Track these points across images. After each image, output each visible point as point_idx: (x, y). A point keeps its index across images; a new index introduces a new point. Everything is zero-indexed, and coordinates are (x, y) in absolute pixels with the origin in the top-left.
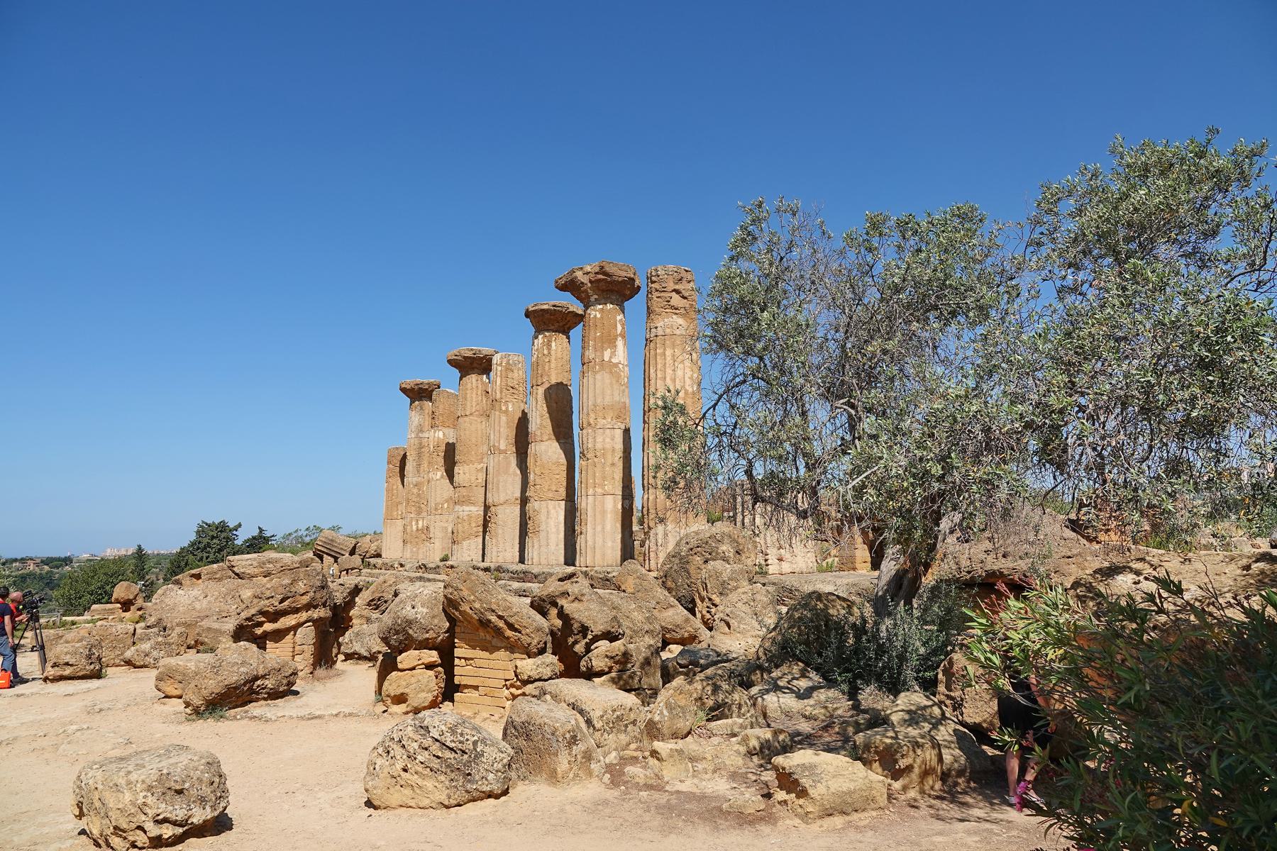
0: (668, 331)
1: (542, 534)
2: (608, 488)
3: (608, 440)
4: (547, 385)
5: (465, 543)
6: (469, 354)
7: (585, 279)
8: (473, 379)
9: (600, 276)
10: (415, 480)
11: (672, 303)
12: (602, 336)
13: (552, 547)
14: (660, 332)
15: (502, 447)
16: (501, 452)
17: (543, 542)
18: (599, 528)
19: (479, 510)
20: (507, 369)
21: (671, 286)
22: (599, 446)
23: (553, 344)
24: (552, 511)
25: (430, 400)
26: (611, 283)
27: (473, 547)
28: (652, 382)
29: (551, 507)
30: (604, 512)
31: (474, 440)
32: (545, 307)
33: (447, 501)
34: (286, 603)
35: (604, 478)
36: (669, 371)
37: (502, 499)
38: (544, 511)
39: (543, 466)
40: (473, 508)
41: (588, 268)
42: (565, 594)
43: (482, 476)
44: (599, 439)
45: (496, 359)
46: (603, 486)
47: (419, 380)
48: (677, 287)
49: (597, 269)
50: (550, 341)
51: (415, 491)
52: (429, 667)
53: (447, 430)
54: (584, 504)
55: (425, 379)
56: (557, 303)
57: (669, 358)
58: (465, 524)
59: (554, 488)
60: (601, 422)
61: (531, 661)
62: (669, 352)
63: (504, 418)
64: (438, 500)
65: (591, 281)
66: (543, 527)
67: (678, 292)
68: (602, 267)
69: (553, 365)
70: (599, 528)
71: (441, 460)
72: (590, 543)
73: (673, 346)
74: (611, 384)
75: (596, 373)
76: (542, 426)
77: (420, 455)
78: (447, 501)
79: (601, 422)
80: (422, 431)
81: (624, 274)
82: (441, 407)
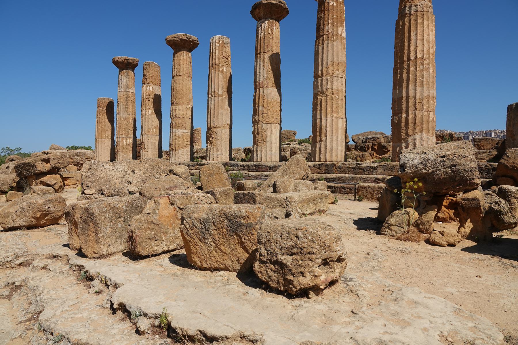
1: (268, 144)
3: (340, 84)
4: (270, 53)
5: (180, 151)
6: (184, 37)
8: (184, 56)
10: (124, 116)
12: (337, 18)
13: (273, 151)
14: (419, 9)
15: (220, 93)
17: (268, 149)
18: (334, 138)
19: (187, 132)
20: (222, 46)
22: (335, 88)
23: (274, 28)
24: (274, 130)
25: (133, 70)
27: (185, 153)
28: (413, 42)
29: (273, 127)
30: (337, 129)
31: (185, 90)
32: (274, 2)
35: (337, 108)
36: (426, 36)
37: (220, 125)
38: (269, 130)
39: (268, 103)
40: (185, 131)
43: (190, 113)
44: (335, 83)
46: (337, 113)
47: (127, 57)
50: (272, 26)
51: (125, 122)
53: (154, 86)
54: (323, 123)
57: (425, 27)
58: (181, 140)
62: (426, 23)
64: (150, 127)
66: (268, 139)
69: (274, 41)
70: (334, 138)
71: (151, 104)
72: (328, 147)
74: (341, 49)
75: (333, 41)
76: (267, 78)
77: (127, 102)
79: (336, 73)
80: (128, 88)
82: (151, 72)
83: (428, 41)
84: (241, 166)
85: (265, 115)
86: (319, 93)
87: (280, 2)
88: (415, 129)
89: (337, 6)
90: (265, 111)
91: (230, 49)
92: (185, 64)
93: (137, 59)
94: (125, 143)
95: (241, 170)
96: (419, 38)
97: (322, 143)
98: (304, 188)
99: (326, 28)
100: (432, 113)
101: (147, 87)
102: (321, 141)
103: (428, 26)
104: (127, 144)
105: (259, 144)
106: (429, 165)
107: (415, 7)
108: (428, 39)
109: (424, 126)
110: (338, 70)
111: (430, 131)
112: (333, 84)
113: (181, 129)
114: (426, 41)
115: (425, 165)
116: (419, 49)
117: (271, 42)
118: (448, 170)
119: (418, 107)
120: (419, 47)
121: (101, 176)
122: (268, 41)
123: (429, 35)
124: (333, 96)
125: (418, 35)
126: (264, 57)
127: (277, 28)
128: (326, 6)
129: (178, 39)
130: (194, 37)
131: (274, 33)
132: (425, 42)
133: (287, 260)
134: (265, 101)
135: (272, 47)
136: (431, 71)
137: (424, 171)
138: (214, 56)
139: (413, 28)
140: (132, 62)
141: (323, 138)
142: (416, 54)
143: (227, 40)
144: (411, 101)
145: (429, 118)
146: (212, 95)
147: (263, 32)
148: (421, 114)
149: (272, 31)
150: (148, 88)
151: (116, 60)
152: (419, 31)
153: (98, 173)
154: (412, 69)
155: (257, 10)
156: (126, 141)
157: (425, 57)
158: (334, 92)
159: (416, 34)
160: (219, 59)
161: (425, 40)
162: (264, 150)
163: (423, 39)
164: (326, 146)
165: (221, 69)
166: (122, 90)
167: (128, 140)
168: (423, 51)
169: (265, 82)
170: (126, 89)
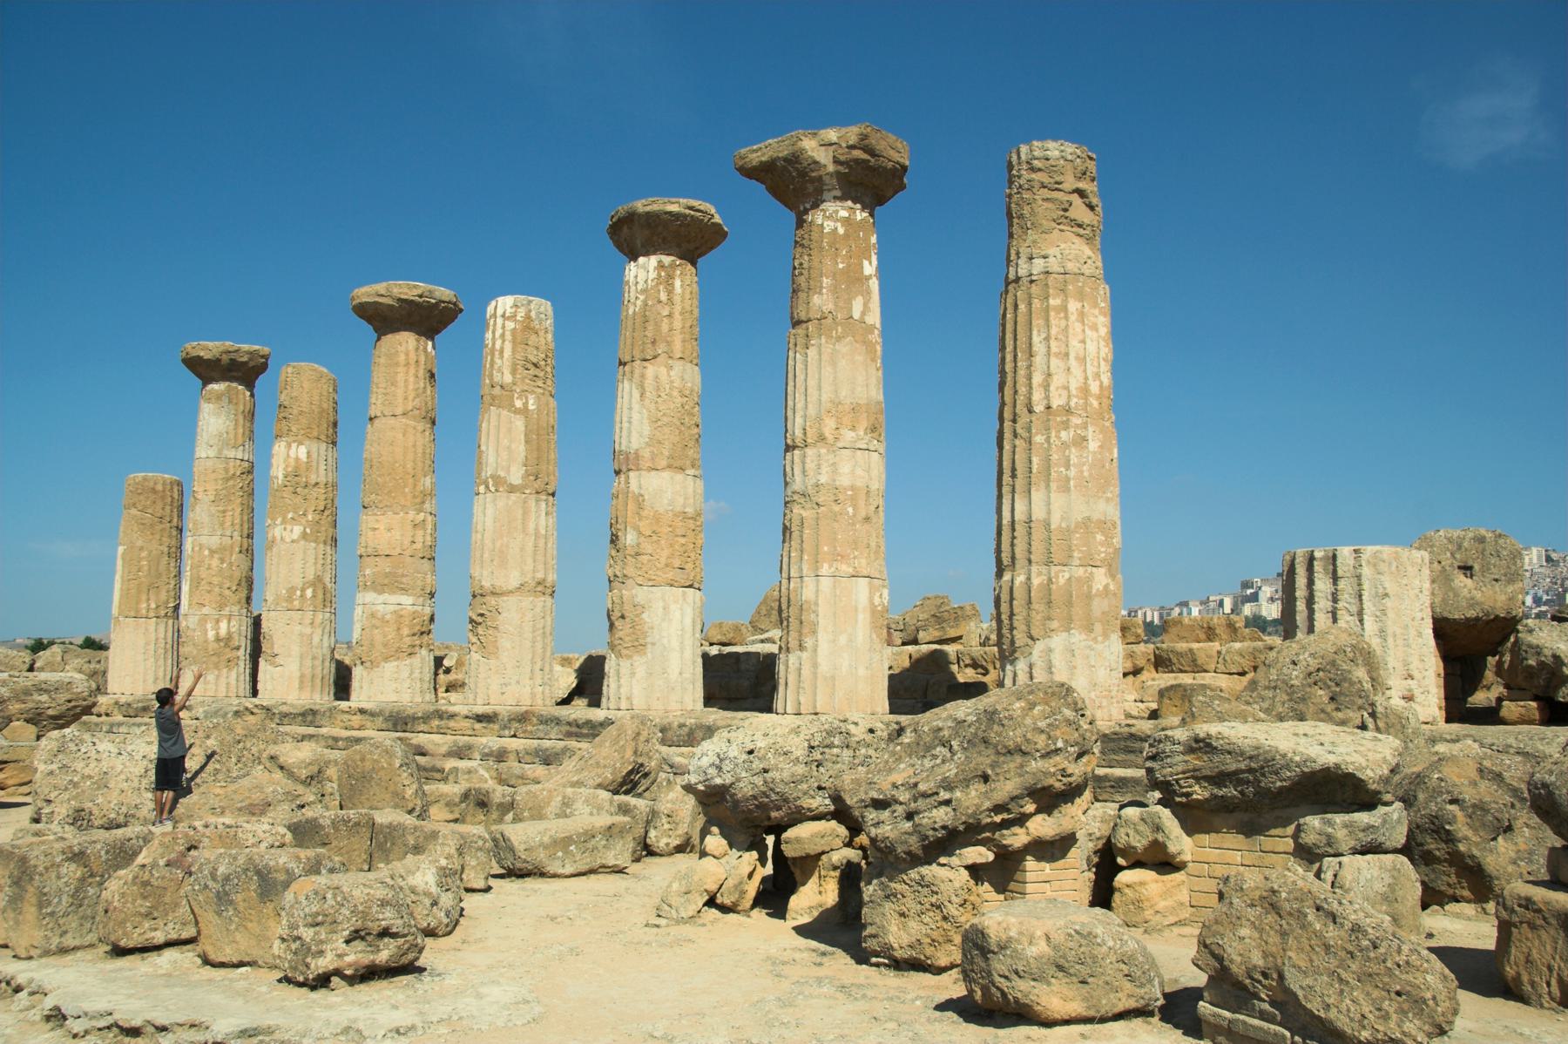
0: (1070, 266)
2: (862, 564)
3: (859, 472)
7: (824, 157)
9: (858, 154)
11: (1071, 214)
16: (512, 489)
21: (1070, 183)
23: (678, 283)
24: (673, 607)
26: (874, 170)
28: (1039, 360)
33: (313, 584)
36: (1075, 343)
37: (514, 582)
39: (657, 518)
44: (845, 469)
48: (1081, 185)
49: (853, 140)
50: (671, 277)
53: (314, 446)
56: (695, 203)
57: (1073, 318)
59: (677, 563)
60: (848, 436)
62: (1073, 306)
63: (519, 423)
65: (836, 161)
67: (1081, 193)
68: (864, 137)
69: (677, 324)
73: (1081, 296)
78: (313, 584)
83: (1082, 360)
84: (569, 724)
85: (645, 558)
86: (796, 497)
87: (691, 208)
88: (1049, 619)
89: (847, 236)
90: (647, 547)
91: (550, 337)
92: (412, 379)
93: (266, 350)
94: (211, 634)
95: (569, 735)
96: (1054, 349)
98: (588, 810)
99: (816, 300)
100: (1102, 570)
101: (289, 446)
102: (801, 647)
103: (1082, 315)
104: (218, 639)
105: (624, 652)
106: (725, 768)
107: (1041, 261)
108: (1081, 354)
109: (1078, 611)
110: (853, 428)
111: (1098, 627)
112: (835, 472)
113: (392, 592)
114: (1077, 358)
115: (719, 768)
116: (1057, 381)
117: (665, 327)
118: (759, 781)
119: (1056, 558)
120: (1055, 378)
121: (87, 771)
122: (657, 326)
123: (1083, 342)
124: (837, 508)
125: (1053, 344)
126: (643, 376)
127: (684, 280)
128: (815, 236)
129: (390, 302)
130: (444, 293)
131: (677, 299)
132: (1073, 362)
133: (307, 934)
134: (644, 513)
135: (668, 343)
136: (1093, 445)
137: (718, 781)
138: (499, 362)
139: (1038, 322)
140: (245, 359)
141: (809, 642)
142: (1047, 397)
143: (541, 308)
144: (1038, 535)
145: (1090, 587)
146: (487, 487)
148: (1067, 575)
149: (670, 292)
150: (292, 453)
151: (194, 353)
152: (1054, 331)
153: (79, 765)
154: (1039, 439)
155: (625, 229)
156: (217, 629)
157: (1072, 404)
158: (841, 497)
159: (1047, 339)
160: (514, 372)
161: (1072, 356)
162: (641, 671)
163: (1067, 355)
164: (815, 665)
165: (519, 404)
166: (212, 453)
167: (223, 626)
168: (1067, 388)
169: (646, 453)
170: (220, 451)
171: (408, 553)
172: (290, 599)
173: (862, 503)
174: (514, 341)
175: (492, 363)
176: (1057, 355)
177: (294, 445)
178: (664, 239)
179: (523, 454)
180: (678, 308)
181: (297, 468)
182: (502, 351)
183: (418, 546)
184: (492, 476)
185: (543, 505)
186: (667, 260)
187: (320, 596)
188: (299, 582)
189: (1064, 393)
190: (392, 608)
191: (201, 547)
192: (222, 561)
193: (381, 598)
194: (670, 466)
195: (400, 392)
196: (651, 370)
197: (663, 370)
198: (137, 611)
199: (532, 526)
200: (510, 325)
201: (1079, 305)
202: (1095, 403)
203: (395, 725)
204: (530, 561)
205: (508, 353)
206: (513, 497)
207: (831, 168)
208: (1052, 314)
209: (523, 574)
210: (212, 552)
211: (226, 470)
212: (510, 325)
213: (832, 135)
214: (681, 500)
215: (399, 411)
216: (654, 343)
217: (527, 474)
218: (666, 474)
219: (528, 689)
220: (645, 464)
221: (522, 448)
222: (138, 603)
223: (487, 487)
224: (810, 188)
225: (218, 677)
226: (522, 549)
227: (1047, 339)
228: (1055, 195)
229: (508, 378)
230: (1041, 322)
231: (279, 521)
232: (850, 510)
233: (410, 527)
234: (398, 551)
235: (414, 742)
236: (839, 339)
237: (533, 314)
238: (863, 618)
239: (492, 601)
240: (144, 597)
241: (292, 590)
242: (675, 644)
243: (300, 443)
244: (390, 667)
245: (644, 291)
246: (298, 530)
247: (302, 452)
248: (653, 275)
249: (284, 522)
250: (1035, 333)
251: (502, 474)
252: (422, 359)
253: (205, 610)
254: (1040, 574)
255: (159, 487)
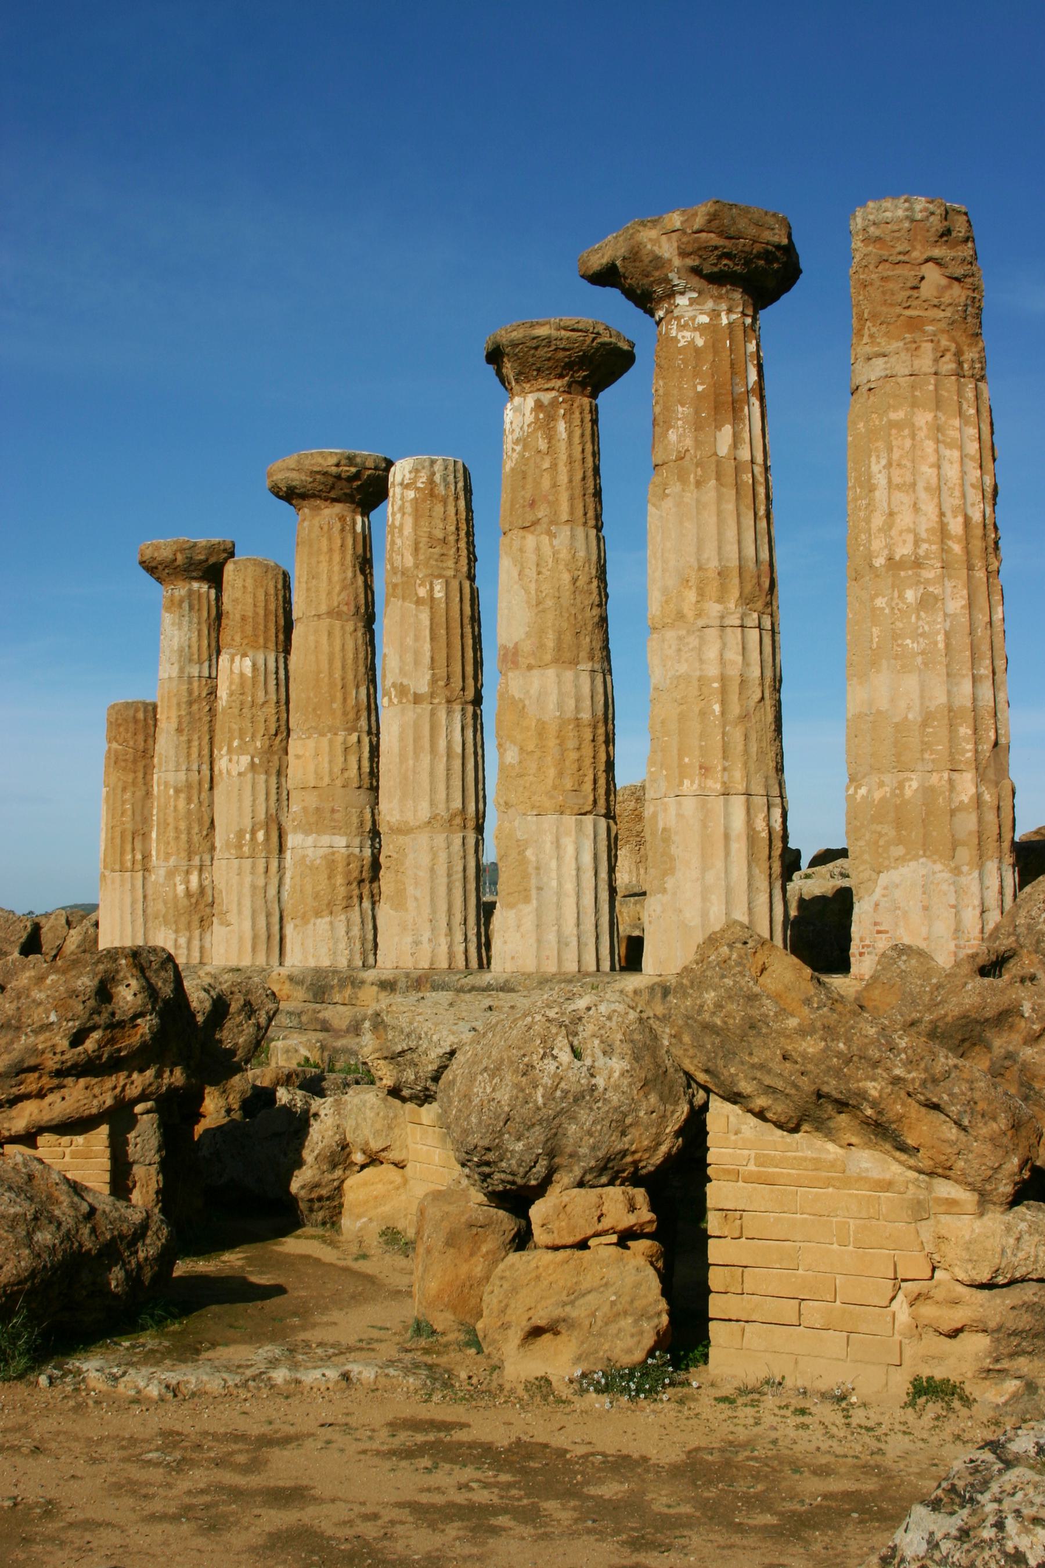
7: (667, 249)
16: (417, 699)
23: (561, 426)
28: (880, 495)
34: (90, 1044)
41: (676, 220)
42: (1005, 1017)
45: (400, 472)
48: (937, 252)
49: (699, 222)
50: (551, 418)
52: (625, 1237)
55: (204, 536)
57: (921, 434)
60: (714, 609)
61: (995, 1220)
63: (425, 617)
65: (683, 254)
68: (713, 217)
81: (767, 236)
92: (336, 568)
94: (181, 889)
96: (896, 480)
97: (665, 898)
102: (664, 891)
104: (188, 894)
110: (720, 600)
114: (927, 489)
120: (898, 519)
122: (537, 484)
138: (398, 541)
146: (390, 699)
147: (518, 448)
148: (915, 785)
149: (550, 438)
152: (896, 456)
156: (187, 882)
161: (921, 485)
163: (914, 485)
169: (527, 647)
170: (182, 670)
171: (339, 783)
172: (239, 846)
173: (734, 697)
174: (417, 516)
175: (393, 543)
176: (898, 487)
177: (237, 658)
178: (538, 370)
179: (428, 654)
180: (563, 457)
181: (242, 685)
182: (401, 528)
183: (353, 772)
184: (394, 685)
185: (458, 716)
186: (546, 397)
187: (275, 838)
188: (247, 823)
189: (910, 538)
190: (321, 852)
191: (166, 784)
192: (189, 800)
193: (310, 840)
194: (556, 661)
195: (324, 585)
196: (530, 540)
197: (545, 539)
198: (122, 863)
199: (442, 744)
200: (411, 494)
201: (929, 416)
202: (957, 548)
203: (315, 996)
204: (441, 787)
205: (408, 530)
206: (419, 709)
207: (677, 262)
208: (894, 431)
209: (432, 803)
210: (177, 791)
211: (190, 692)
212: (411, 494)
213: (676, 220)
214: (571, 703)
215: (323, 609)
216: (533, 504)
217: (434, 681)
218: (551, 672)
219: (444, 949)
220: (523, 661)
221: (427, 646)
222: (122, 853)
223: (390, 699)
224: (659, 290)
225: (189, 942)
226: (432, 774)
227: (889, 464)
228: (899, 270)
229: (409, 561)
230: (880, 444)
231: (225, 749)
232: (717, 708)
233: (339, 750)
234: (327, 780)
235: (321, 1015)
236: (698, 484)
237: (438, 478)
238: (739, 848)
239: (401, 839)
240: (129, 847)
241: (240, 834)
242: (570, 886)
243: (244, 655)
244: (323, 923)
245: (517, 442)
246: (245, 760)
247: (248, 662)
248: (529, 418)
249: (230, 751)
250: (873, 459)
251: (405, 682)
252: (350, 542)
253: (172, 861)
254: (881, 784)
255: (141, 715)
